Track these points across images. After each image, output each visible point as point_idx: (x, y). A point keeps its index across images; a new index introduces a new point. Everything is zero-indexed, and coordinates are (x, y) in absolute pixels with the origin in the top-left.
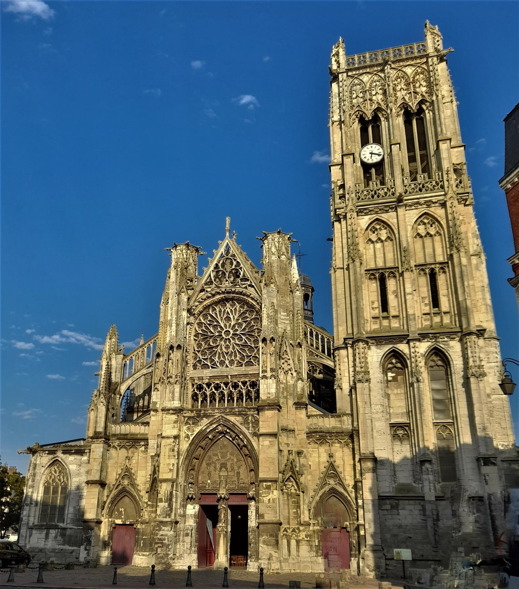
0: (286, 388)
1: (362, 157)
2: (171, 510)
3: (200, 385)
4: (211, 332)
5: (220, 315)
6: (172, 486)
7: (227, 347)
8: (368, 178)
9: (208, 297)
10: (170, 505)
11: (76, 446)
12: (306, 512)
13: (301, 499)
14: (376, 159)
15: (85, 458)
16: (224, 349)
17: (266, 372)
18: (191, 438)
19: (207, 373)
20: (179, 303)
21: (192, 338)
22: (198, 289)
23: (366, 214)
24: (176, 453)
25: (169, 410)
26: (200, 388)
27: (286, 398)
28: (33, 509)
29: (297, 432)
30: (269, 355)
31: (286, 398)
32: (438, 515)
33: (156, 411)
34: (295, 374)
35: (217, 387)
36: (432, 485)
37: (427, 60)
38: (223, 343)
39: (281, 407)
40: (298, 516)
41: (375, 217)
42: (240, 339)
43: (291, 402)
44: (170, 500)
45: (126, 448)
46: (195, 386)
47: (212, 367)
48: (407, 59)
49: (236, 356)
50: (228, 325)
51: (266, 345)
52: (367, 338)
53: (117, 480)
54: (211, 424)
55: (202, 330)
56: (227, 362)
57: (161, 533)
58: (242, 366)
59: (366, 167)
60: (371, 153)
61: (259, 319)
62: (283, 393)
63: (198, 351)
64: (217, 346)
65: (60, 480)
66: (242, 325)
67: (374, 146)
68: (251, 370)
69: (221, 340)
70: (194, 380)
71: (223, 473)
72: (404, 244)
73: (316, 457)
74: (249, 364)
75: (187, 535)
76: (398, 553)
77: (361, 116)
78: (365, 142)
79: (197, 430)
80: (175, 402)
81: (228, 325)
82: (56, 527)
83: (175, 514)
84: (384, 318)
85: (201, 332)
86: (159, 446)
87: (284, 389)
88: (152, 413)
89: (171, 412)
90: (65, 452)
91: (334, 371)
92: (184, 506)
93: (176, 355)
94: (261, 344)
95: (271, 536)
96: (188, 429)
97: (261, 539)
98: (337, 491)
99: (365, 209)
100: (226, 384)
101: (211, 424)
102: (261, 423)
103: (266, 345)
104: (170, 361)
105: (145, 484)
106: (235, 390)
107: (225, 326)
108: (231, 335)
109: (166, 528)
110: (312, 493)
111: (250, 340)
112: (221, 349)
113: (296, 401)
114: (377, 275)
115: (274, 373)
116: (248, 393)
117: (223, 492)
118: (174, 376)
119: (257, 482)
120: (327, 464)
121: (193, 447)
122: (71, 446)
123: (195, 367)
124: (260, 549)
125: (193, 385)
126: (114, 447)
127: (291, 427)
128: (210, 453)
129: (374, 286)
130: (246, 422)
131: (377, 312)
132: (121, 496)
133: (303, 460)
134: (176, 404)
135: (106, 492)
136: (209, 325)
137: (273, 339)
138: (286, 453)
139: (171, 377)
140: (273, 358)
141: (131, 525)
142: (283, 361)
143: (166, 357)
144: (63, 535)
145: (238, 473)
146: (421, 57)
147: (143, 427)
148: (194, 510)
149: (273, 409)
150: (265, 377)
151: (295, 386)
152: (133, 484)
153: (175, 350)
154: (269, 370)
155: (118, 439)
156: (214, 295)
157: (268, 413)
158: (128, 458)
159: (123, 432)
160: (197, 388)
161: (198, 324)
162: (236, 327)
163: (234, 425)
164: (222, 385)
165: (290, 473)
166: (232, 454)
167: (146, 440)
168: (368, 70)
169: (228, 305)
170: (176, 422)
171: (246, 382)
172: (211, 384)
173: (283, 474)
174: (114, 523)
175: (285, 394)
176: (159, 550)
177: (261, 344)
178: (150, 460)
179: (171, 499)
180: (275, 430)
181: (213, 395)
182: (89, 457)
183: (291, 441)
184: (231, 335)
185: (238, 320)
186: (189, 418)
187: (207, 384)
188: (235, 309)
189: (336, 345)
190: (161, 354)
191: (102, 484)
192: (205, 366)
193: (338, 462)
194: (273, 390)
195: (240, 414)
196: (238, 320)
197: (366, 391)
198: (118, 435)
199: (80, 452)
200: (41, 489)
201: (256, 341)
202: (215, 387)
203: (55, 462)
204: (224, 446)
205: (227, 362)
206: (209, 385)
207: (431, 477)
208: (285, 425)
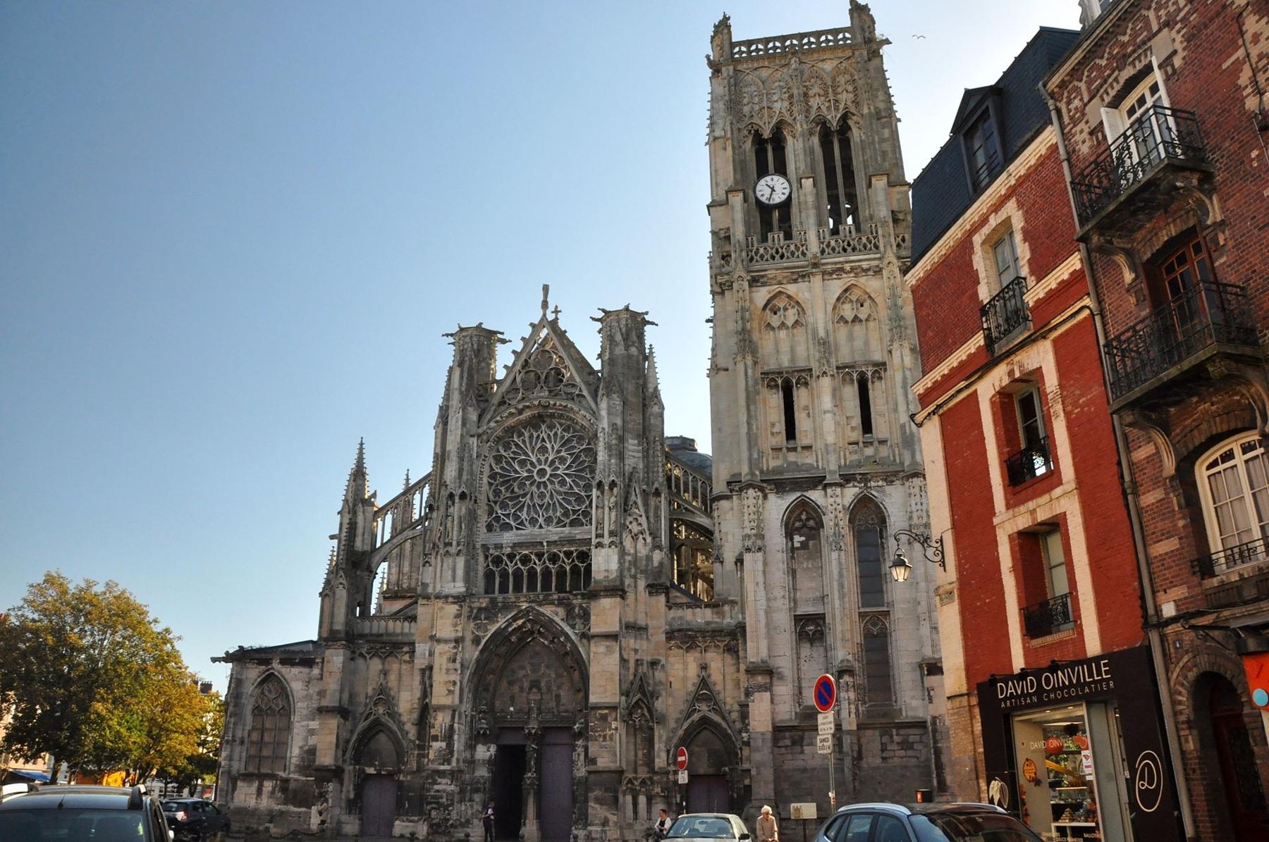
0: (635, 562)
1: (759, 194)
2: (451, 752)
3: (498, 557)
4: (517, 472)
5: (531, 443)
6: (453, 717)
7: (542, 496)
8: (767, 226)
10: (450, 746)
12: (664, 755)
13: (656, 734)
14: (778, 198)
15: (316, 671)
16: (536, 500)
17: (602, 536)
19: (508, 538)
20: (464, 424)
21: (485, 480)
22: (495, 401)
23: (764, 284)
24: (458, 665)
25: (446, 597)
26: (497, 561)
27: (634, 577)
28: (237, 749)
29: (650, 631)
30: (607, 509)
31: (634, 577)
32: (860, 752)
33: (427, 597)
34: (649, 540)
35: (525, 560)
36: (853, 707)
38: (534, 488)
39: (624, 592)
40: (650, 762)
41: (777, 288)
42: (563, 483)
43: (642, 584)
44: (449, 736)
45: (380, 657)
49: (555, 511)
50: (543, 458)
51: (603, 493)
52: (762, 481)
53: (366, 705)
54: (515, 619)
55: (502, 468)
56: (541, 520)
57: (436, 787)
58: (564, 526)
59: (764, 209)
61: (592, 453)
62: (629, 569)
64: (524, 495)
65: (277, 705)
66: (565, 459)
67: (776, 178)
68: (578, 533)
69: (532, 484)
70: (488, 549)
71: (534, 696)
72: (822, 333)
73: (682, 671)
74: (573, 523)
75: (477, 790)
76: (797, 810)
78: (762, 172)
79: (493, 629)
80: (458, 584)
81: (543, 458)
82: (272, 777)
83: (458, 760)
84: (789, 450)
86: (431, 654)
87: (631, 565)
88: (420, 601)
89: (450, 600)
90: (283, 662)
91: (712, 533)
92: (471, 747)
93: (458, 509)
94: (595, 492)
95: (606, 790)
96: (478, 627)
97: (592, 795)
98: (711, 720)
99: (763, 276)
100: (540, 556)
101: (515, 619)
102: (593, 618)
105: (411, 712)
107: (539, 461)
109: (444, 781)
110: (672, 724)
111: (578, 485)
112: (532, 499)
113: (650, 582)
114: (780, 382)
115: (614, 539)
116: (575, 570)
117: (533, 726)
118: (454, 543)
119: (586, 708)
120: (696, 681)
123: (490, 528)
124: (590, 810)
125: (486, 557)
126: (361, 655)
127: (641, 622)
128: (514, 665)
129: (775, 400)
130: (570, 616)
131: (781, 439)
133: (659, 675)
134: (459, 587)
135: (349, 725)
136: (514, 459)
137: (613, 485)
138: (632, 664)
139: (451, 544)
140: (613, 514)
141: (390, 775)
142: (630, 519)
143: (442, 509)
144: (284, 790)
145: (558, 696)
147: (406, 624)
149: (611, 596)
150: (599, 545)
151: (649, 558)
152: (393, 715)
153: (457, 499)
155: (368, 641)
156: (520, 412)
157: (606, 602)
158: (385, 673)
159: (375, 631)
160: (493, 562)
161: (495, 457)
164: (533, 557)
165: (639, 696)
166: (547, 667)
167: (413, 644)
170: (458, 616)
173: (627, 696)
175: (633, 570)
176: (434, 813)
177: (595, 492)
178: (417, 678)
180: (614, 627)
181: (518, 575)
182: (322, 669)
183: (642, 645)
185: (559, 451)
186: (480, 609)
188: (556, 434)
189: (716, 491)
190: (435, 506)
191: (342, 712)
192: (507, 527)
193: (716, 676)
194: (614, 566)
195: (560, 603)
196: (559, 451)
197: (760, 566)
198: (366, 635)
199: (308, 662)
200: (249, 719)
201: (588, 487)
203: (269, 678)
204: (537, 654)
205: (541, 520)
206: (511, 557)
207: (852, 695)
208: (632, 620)
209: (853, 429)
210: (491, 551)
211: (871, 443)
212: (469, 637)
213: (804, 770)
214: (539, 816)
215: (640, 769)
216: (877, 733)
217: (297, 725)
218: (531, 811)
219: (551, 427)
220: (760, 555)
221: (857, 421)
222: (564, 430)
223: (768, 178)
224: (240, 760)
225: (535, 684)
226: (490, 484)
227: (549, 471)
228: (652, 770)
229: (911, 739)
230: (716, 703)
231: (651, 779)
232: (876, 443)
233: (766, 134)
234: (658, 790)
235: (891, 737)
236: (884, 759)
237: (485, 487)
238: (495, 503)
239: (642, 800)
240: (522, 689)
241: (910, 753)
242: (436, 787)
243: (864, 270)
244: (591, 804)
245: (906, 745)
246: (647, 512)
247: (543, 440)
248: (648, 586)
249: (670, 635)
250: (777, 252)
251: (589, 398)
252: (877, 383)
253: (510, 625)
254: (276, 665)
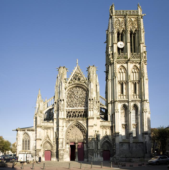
2: (63, 147)
4: (72, 97)
6: (63, 140)
9: (71, 85)
10: (63, 145)
11: (31, 129)
12: (99, 147)
14: (122, 47)
18: (68, 127)
23: (119, 64)
25: (61, 118)
26: (69, 112)
34: (97, 110)
37: (138, 17)
38: (76, 100)
41: (121, 65)
43: (96, 117)
44: (62, 144)
46: (67, 112)
47: (73, 107)
48: (132, 15)
51: (90, 101)
57: (60, 152)
59: (119, 49)
60: (121, 45)
63: (68, 102)
65: (27, 138)
77: (118, 32)
79: (69, 124)
89: (61, 119)
90: (28, 130)
99: (119, 62)
103: (90, 101)
104: (61, 104)
106: (79, 113)
108: (78, 98)
118: (62, 109)
121: (68, 129)
122: (30, 129)
123: (67, 107)
125: (67, 112)
127: (96, 124)
132: (46, 143)
142: (94, 106)
145: (81, 137)
146: (136, 15)
148: (69, 146)
154: (91, 109)
163: (80, 123)
164: (76, 112)
168: (121, 16)
169: (77, 88)
170: (63, 122)
171: (83, 111)
172: (72, 112)
174: (45, 150)
179: (63, 143)
180: (93, 125)
184: (78, 98)
187: (71, 112)
202: (73, 113)
205: (77, 106)
206: (71, 112)
210: (67, 111)
212: (65, 126)
213: (123, 149)
214: (78, 157)
215: (96, 149)
216: (135, 144)
217: (31, 142)
218: (77, 157)
220: (118, 113)
224: (20, 148)
225: (76, 135)
226: (67, 99)
227: (78, 97)
228: (98, 149)
229: (140, 145)
230: (109, 138)
231: (97, 151)
234: (99, 152)
235: (137, 145)
236: (136, 148)
237: (66, 99)
238: (68, 102)
239: (96, 154)
240: (74, 135)
241: (140, 147)
242: (60, 152)
243: (137, 62)
244: (89, 155)
245: (140, 146)
246: (97, 105)
248: (97, 118)
249: (101, 126)
253: (72, 124)
254: (26, 131)
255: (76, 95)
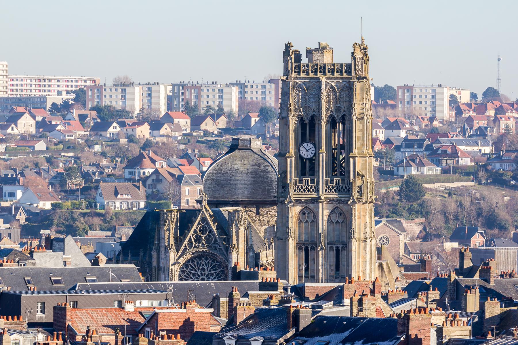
50: (203, 273)
55: (185, 276)
66: (213, 274)
85: (184, 277)
162: (209, 276)
185: (210, 271)
188: (208, 263)
196: (210, 271)
209: (332, 270)
211: (339, 277)
219: (206, 259)
221: (334, 268)
222: (212, 261)
223: (305, 144)
232: (340, 278)
233: (307, 121)
247: (203, 265)
250: (307, 188)
251: (224, 250)
252: (343, 251)
255: (199, 274)
